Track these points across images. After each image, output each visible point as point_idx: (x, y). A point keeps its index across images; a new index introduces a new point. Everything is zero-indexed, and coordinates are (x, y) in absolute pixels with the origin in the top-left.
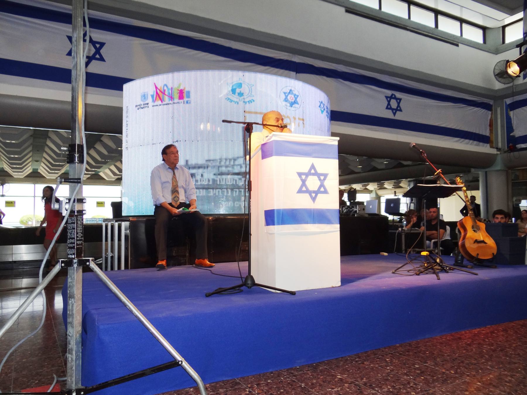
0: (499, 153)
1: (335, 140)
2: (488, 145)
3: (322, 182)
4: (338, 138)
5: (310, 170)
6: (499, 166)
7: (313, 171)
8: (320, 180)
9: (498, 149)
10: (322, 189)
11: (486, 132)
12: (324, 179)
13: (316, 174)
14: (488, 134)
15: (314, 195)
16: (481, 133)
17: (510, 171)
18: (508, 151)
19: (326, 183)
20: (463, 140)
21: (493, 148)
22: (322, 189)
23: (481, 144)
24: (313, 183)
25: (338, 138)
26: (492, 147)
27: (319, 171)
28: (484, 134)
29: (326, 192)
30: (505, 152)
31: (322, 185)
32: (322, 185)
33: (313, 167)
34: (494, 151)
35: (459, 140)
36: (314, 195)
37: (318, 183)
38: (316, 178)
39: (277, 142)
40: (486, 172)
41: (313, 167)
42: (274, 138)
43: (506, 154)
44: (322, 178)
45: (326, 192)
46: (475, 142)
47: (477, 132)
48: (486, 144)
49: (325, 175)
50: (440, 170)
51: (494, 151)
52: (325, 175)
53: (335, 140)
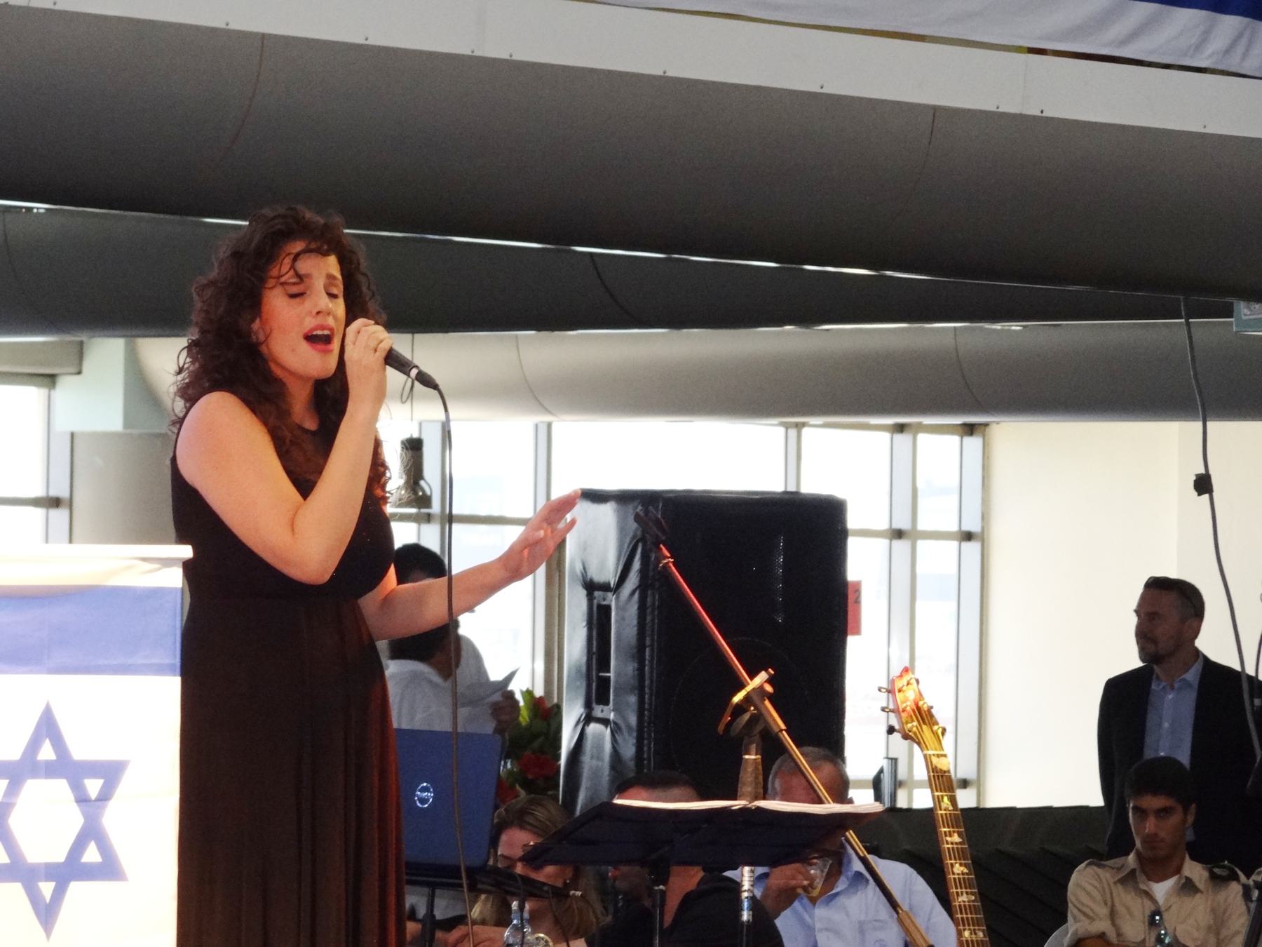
1: (167, 562)
3: (91, 807)
4: (186, 551)
5: (34, 745)
7: (47, 753)
8: (82, 799)
10: (92, 855)
12: (105, 796)
13: (68, 769)
15: (47, 888)
19: (113, 819)
22: (92, 855)
24: (45, 821)
25: (186, 551)
27: (80, 751)
29: (109, 869)
31: (91, 832)
32: (91, 832)
33: (48, 727)
36: (47, 888)
37: (74, 820)
38: (61, 787)
41: (48, 727)
44: (93, 787)
45: (109, 869)
49: (111, 772)
50: (762, 677)
52: (111, 772)
53: (167, 562)
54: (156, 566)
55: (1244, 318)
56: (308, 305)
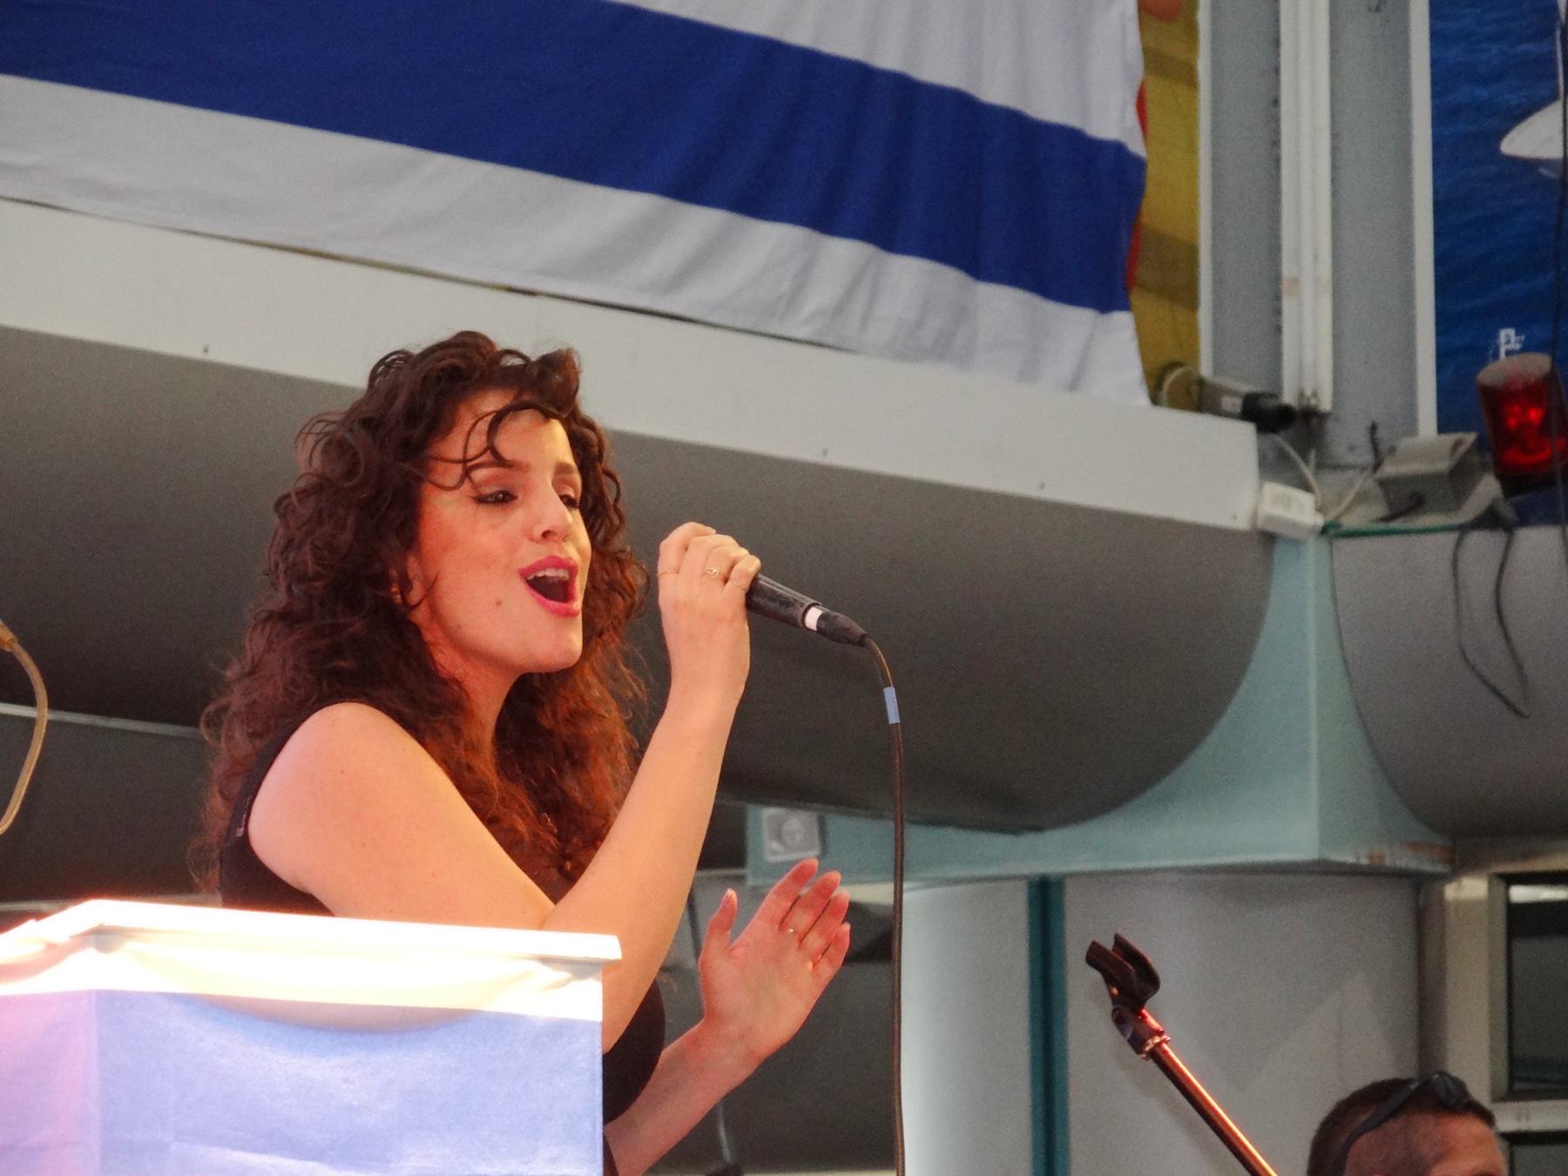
0: (1297, 508)
1: (581, 968)
2: (1111, 343)
6: (1279, 793)
9: (1288, 430)
11: (1082, 81)
14: (1110, 118)
16: (995, 91)
17: (1471, 888)
18: (1459, 478)
20: (700, 222)
21: (1198, 398)
23: (1001, 306)
26: (1176, 385)
28: (1049, 107)
30: (1407, 500)
34: (1210, 477)
35: (640, 238)
39: (112, 1004)
40: (1045, 897)
42: (89, 972)
43: (1427, 549)
46: (910, 279)
47: (938, 68)
48: (1075, 322)
51: (1210, 477)
53: (581, 968)
54: (564, 975)
55: (772, 859)
56: (517, 517)
